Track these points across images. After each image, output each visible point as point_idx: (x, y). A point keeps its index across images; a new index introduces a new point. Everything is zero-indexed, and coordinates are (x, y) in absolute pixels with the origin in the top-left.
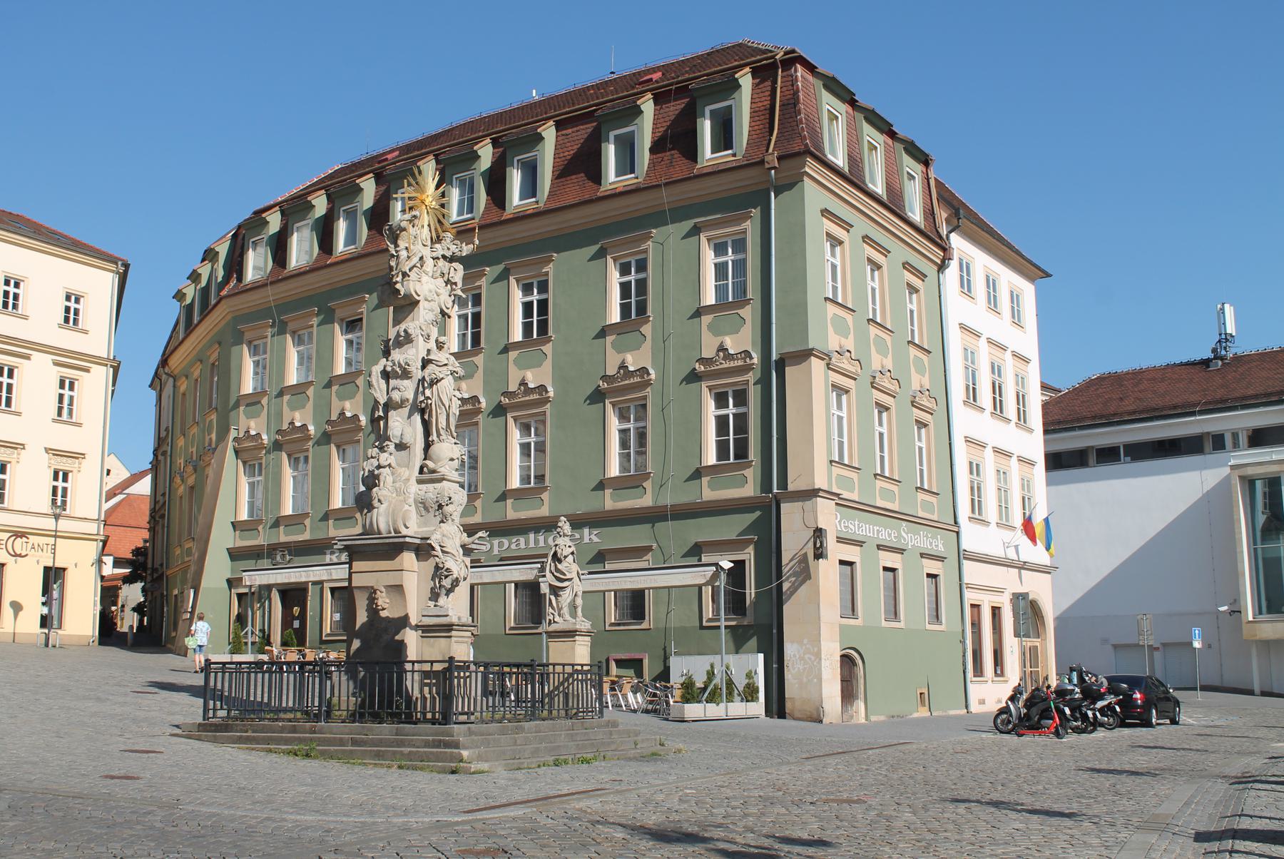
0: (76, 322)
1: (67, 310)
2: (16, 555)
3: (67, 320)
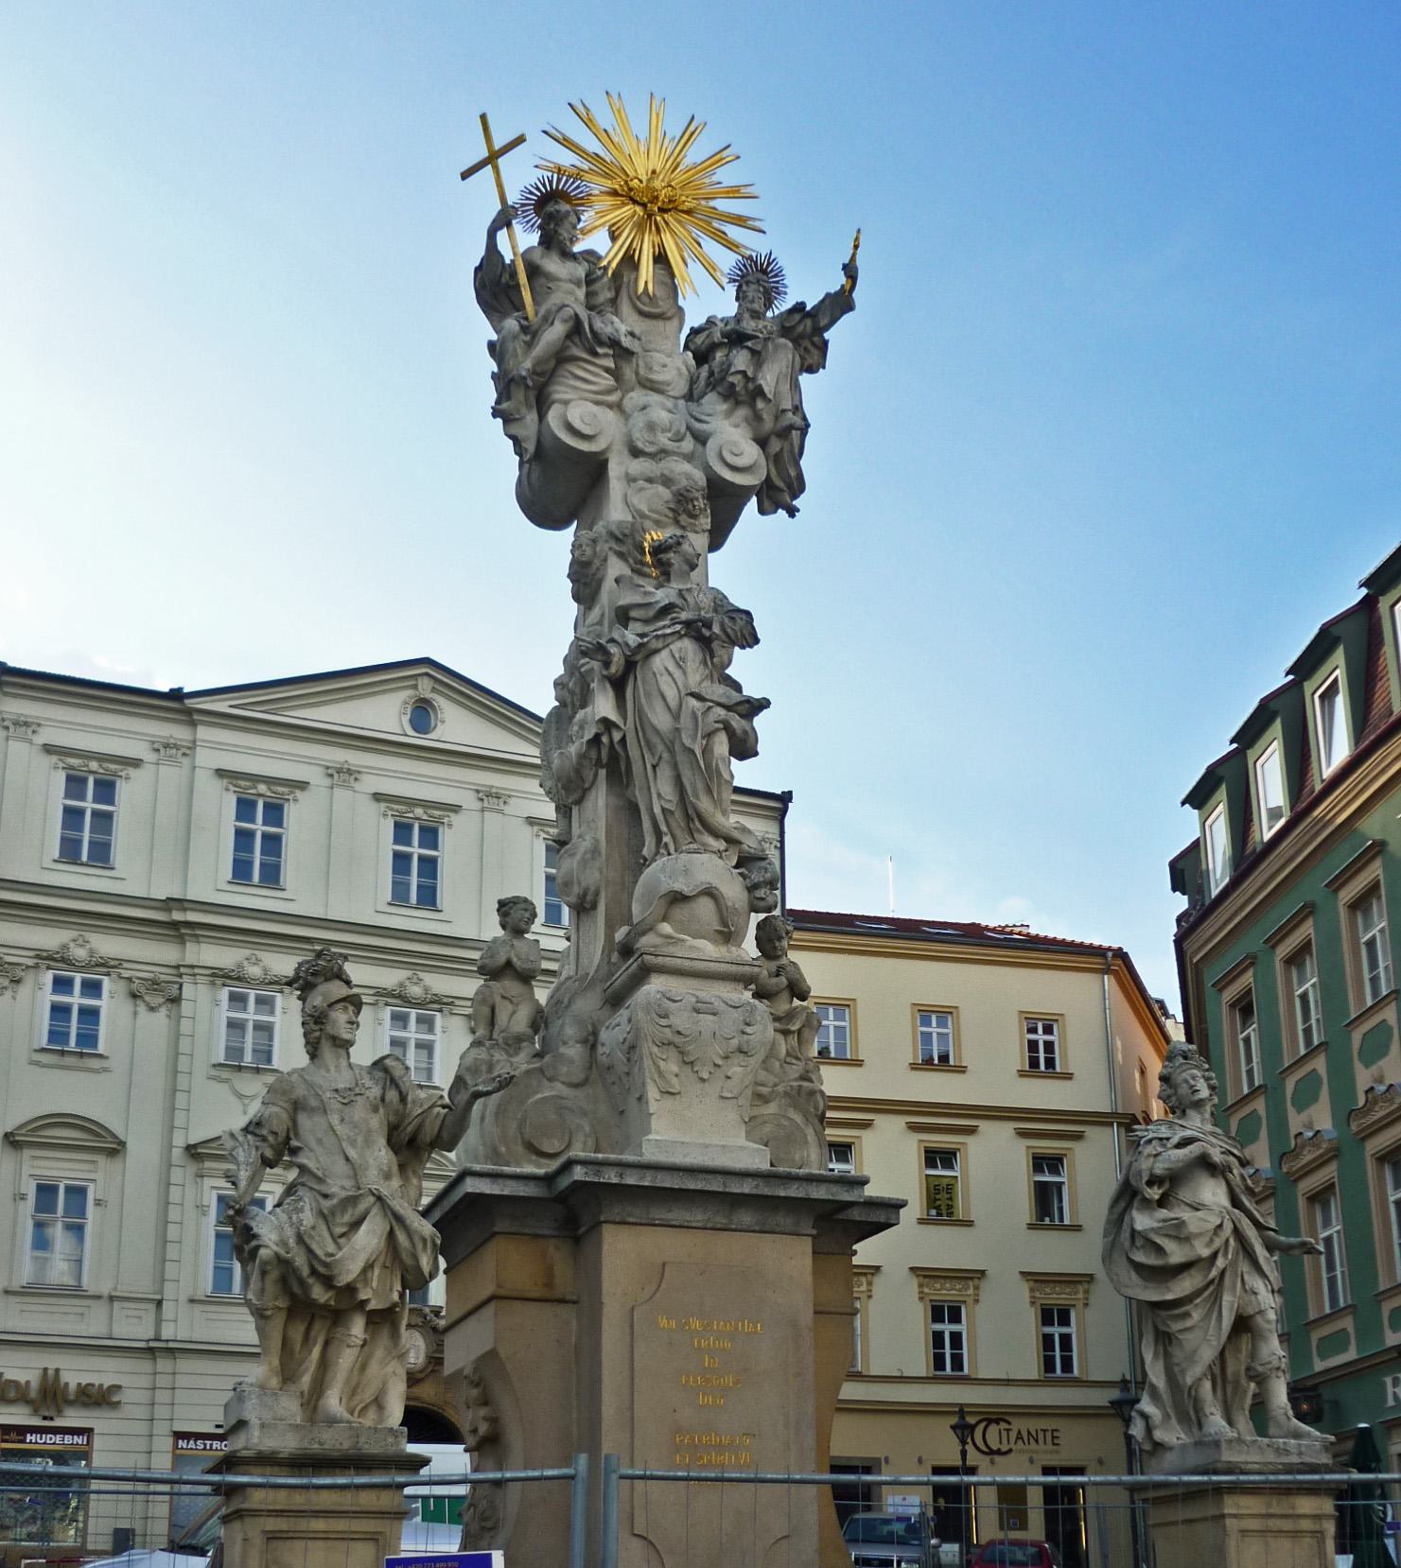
0: (1050, 1063)
1: (1033, 1046)
2: (991, 1452)
3: (1034, 1063)
